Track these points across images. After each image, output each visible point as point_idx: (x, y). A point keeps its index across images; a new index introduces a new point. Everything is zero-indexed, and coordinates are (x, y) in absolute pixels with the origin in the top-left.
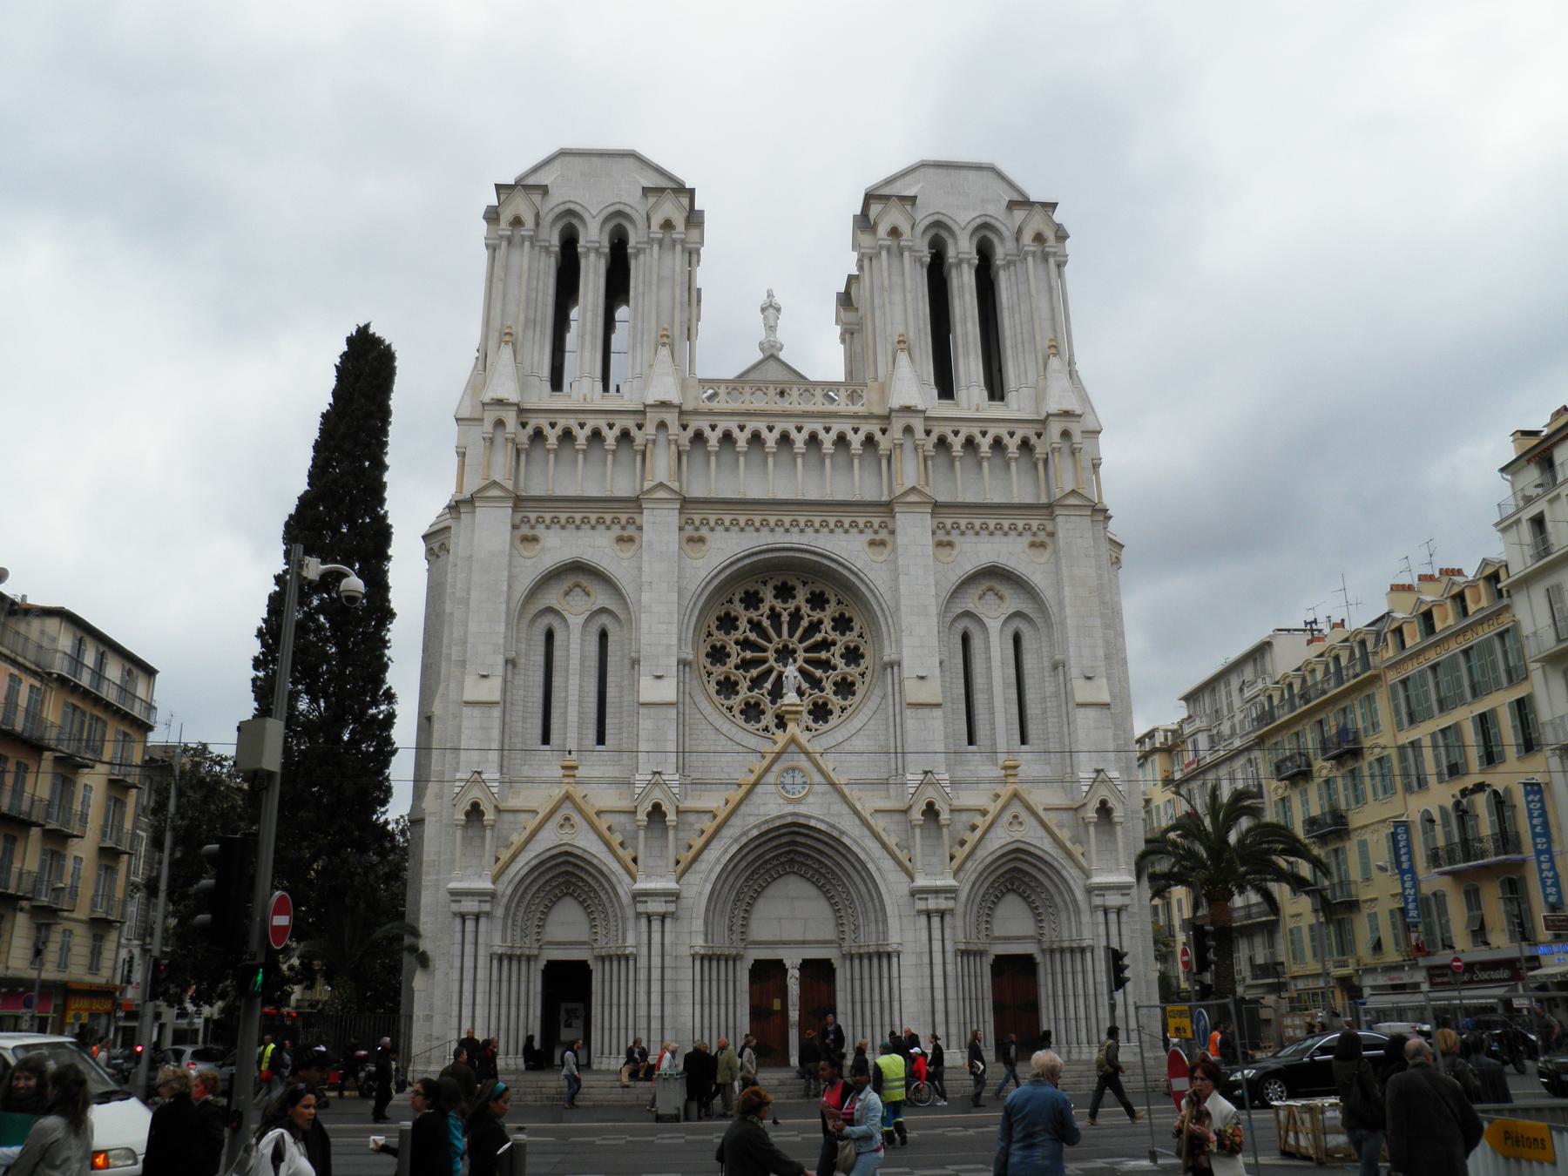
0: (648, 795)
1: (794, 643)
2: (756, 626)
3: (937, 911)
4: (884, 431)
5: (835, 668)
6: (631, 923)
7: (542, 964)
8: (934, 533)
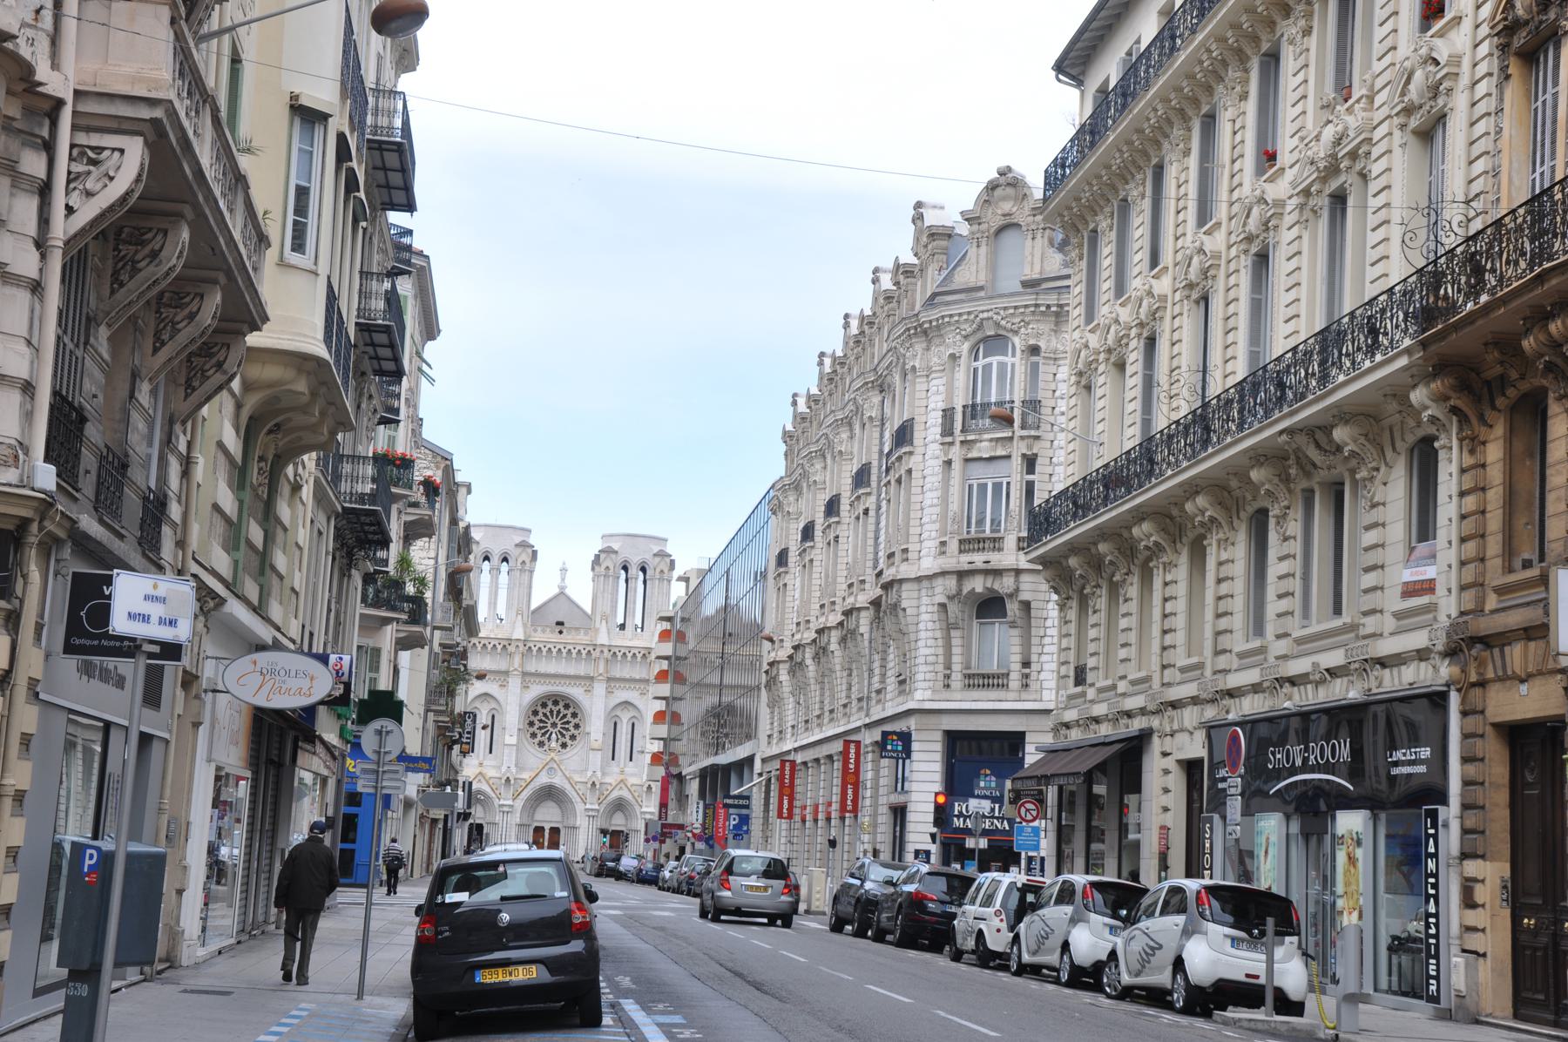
2: (545, 715)
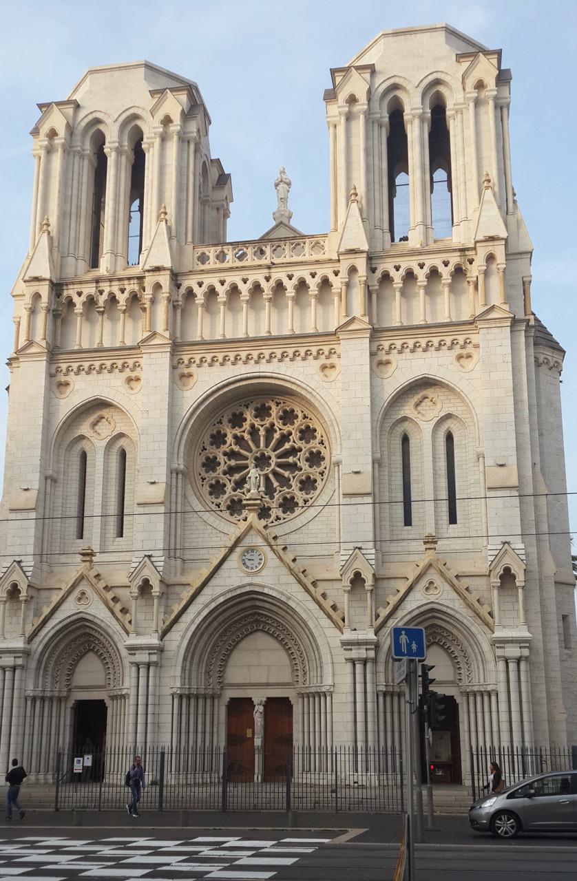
0: (139, 573)
1: (269, 452)
5: (300, 469)
7: (71, 703)
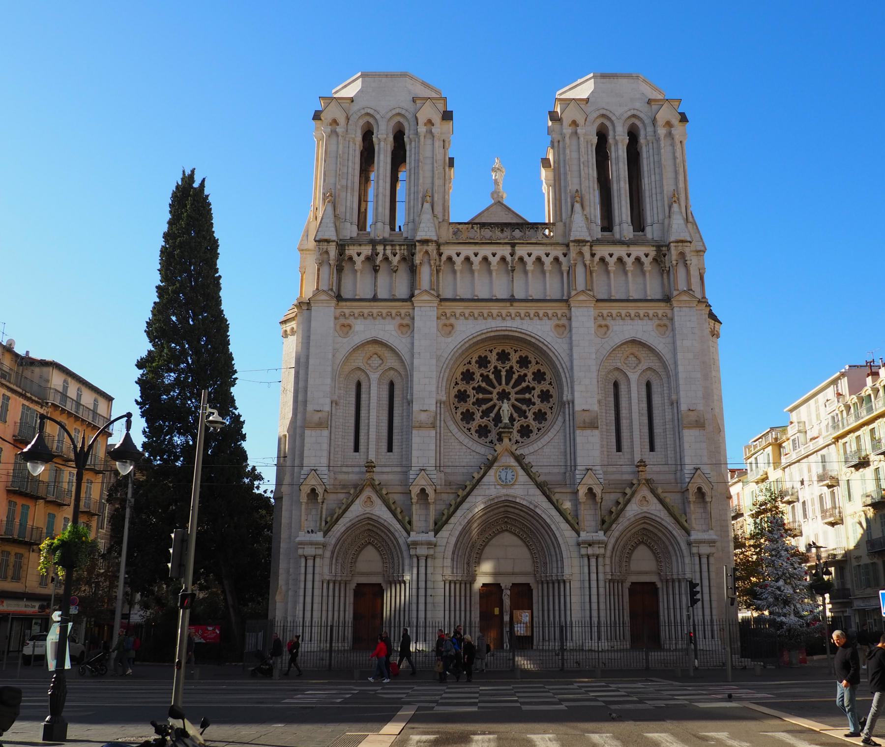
1: (508, 389)
3: (593, 555)
4: (565, 255)
6: (407, 562)
8: (595, 319)
